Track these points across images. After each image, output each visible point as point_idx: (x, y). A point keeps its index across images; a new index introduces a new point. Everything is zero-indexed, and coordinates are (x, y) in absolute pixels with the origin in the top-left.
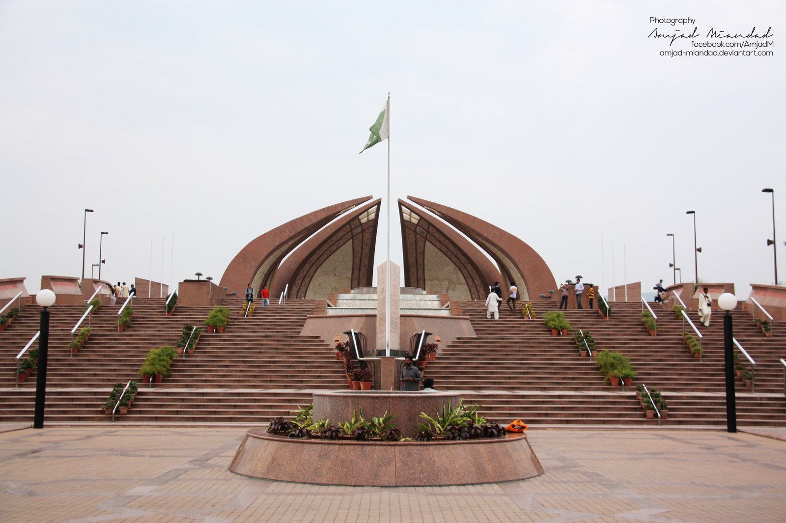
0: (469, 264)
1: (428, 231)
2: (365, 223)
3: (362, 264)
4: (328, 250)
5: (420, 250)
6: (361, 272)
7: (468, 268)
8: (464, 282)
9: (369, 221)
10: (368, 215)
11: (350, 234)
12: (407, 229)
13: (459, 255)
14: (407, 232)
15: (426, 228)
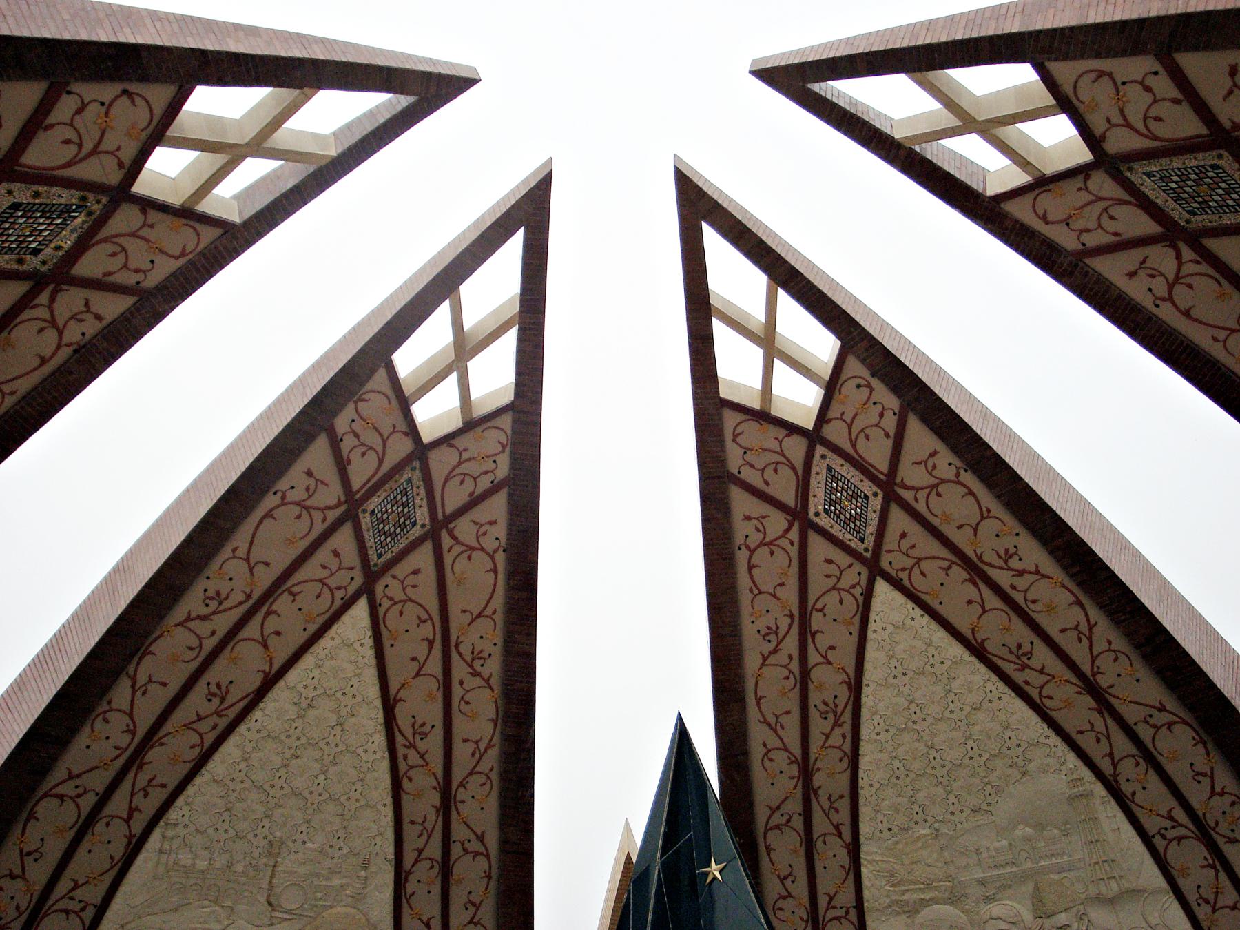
0: (1178, 728)
1: (889, 486)
2: (446, 440)
3: (459, 832)
4: (200, 689)
5: (828, 683)
6: (458, 896)
7: (1169, 768)
8: (1151, 875)
9: (472, 424)
10: (465, 348)
11: (344, 539)
12: (741, 503)
13: (1105, 662)
14: (742, 530)
15: (877, 453)
